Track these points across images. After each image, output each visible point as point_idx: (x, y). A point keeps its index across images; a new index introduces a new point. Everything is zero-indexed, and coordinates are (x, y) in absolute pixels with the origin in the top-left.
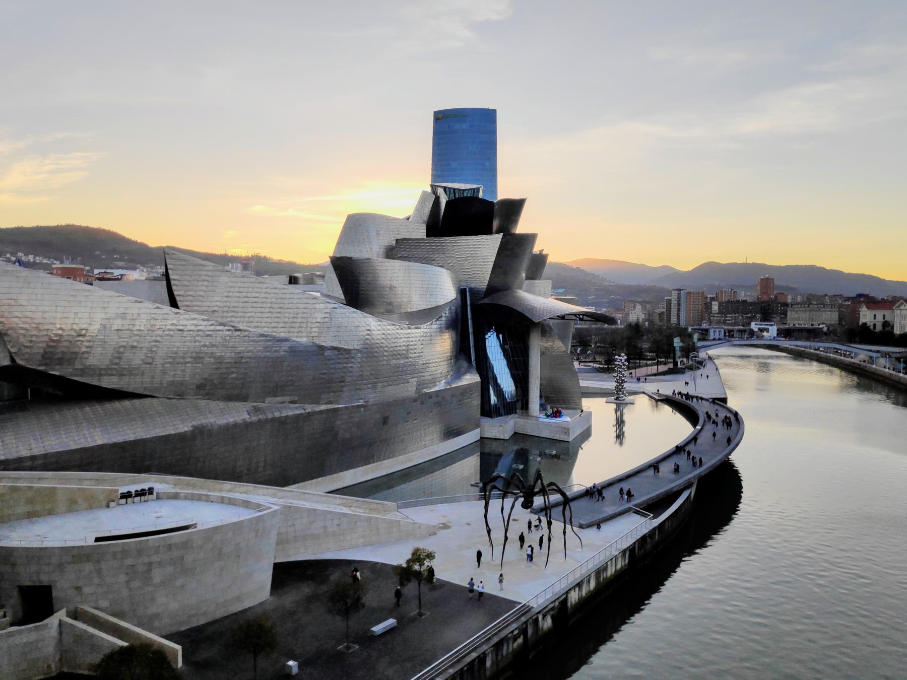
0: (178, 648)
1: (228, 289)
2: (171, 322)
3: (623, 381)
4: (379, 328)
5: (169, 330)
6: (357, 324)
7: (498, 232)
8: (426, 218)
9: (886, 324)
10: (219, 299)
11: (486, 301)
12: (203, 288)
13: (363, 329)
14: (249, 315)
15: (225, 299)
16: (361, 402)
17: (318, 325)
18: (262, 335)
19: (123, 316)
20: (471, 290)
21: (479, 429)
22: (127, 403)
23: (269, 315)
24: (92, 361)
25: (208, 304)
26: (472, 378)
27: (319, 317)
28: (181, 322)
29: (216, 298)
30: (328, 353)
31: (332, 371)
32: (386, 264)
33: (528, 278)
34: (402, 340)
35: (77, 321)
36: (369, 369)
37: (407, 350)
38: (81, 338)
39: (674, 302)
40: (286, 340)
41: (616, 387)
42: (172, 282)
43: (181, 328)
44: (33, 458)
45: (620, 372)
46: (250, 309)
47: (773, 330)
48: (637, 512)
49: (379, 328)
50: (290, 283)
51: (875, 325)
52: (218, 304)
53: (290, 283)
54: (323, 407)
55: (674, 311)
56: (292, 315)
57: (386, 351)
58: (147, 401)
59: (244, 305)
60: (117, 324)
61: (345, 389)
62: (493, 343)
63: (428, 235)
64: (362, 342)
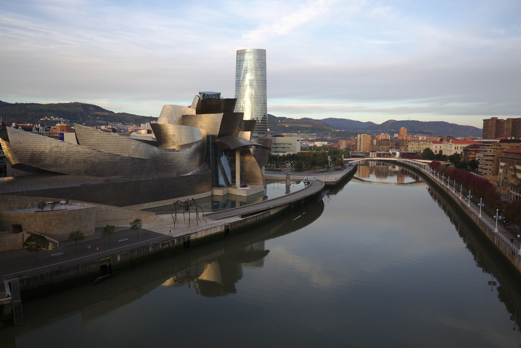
0: (57, 242)
9: (441, 151)
11: (218, 140)
16: (150, 179)
18: (109, 154)
19: (57, 147)
22: (59, 177)
24: (47, 162)
27: (133, 147)
30: (136, 160)
40: (119, 155)
44: (23, 192)
47: (398, 154)
50: (148, 133)
53: (148, 133)
55: (358, 144)
58: (66, 176)
60: (55, 149)
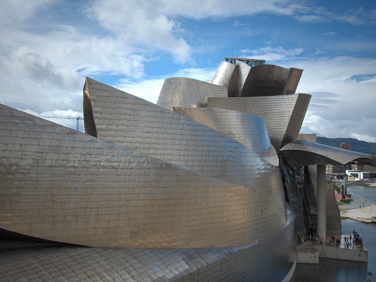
1: (148, 124)
2: (104, 158)
5: (104, 167)
8: (227, 83)
10: (141, 134)
12: (125, 122)
14: (168, 152)
15: (146, 135)
23: (186, 152)
25: (130, 139)
28: (115, 159)
29: (137, 134)
32: (225, 114)
35: (7, 154)
38: (11, 176)
42: (95, 115)
43: (115, 164)
46: (170, 147)
47: (361, 175)
49: (263, 167)
52: (140, 139)
56: (205, 153)
59: (165, 141)
63: (228, 96)
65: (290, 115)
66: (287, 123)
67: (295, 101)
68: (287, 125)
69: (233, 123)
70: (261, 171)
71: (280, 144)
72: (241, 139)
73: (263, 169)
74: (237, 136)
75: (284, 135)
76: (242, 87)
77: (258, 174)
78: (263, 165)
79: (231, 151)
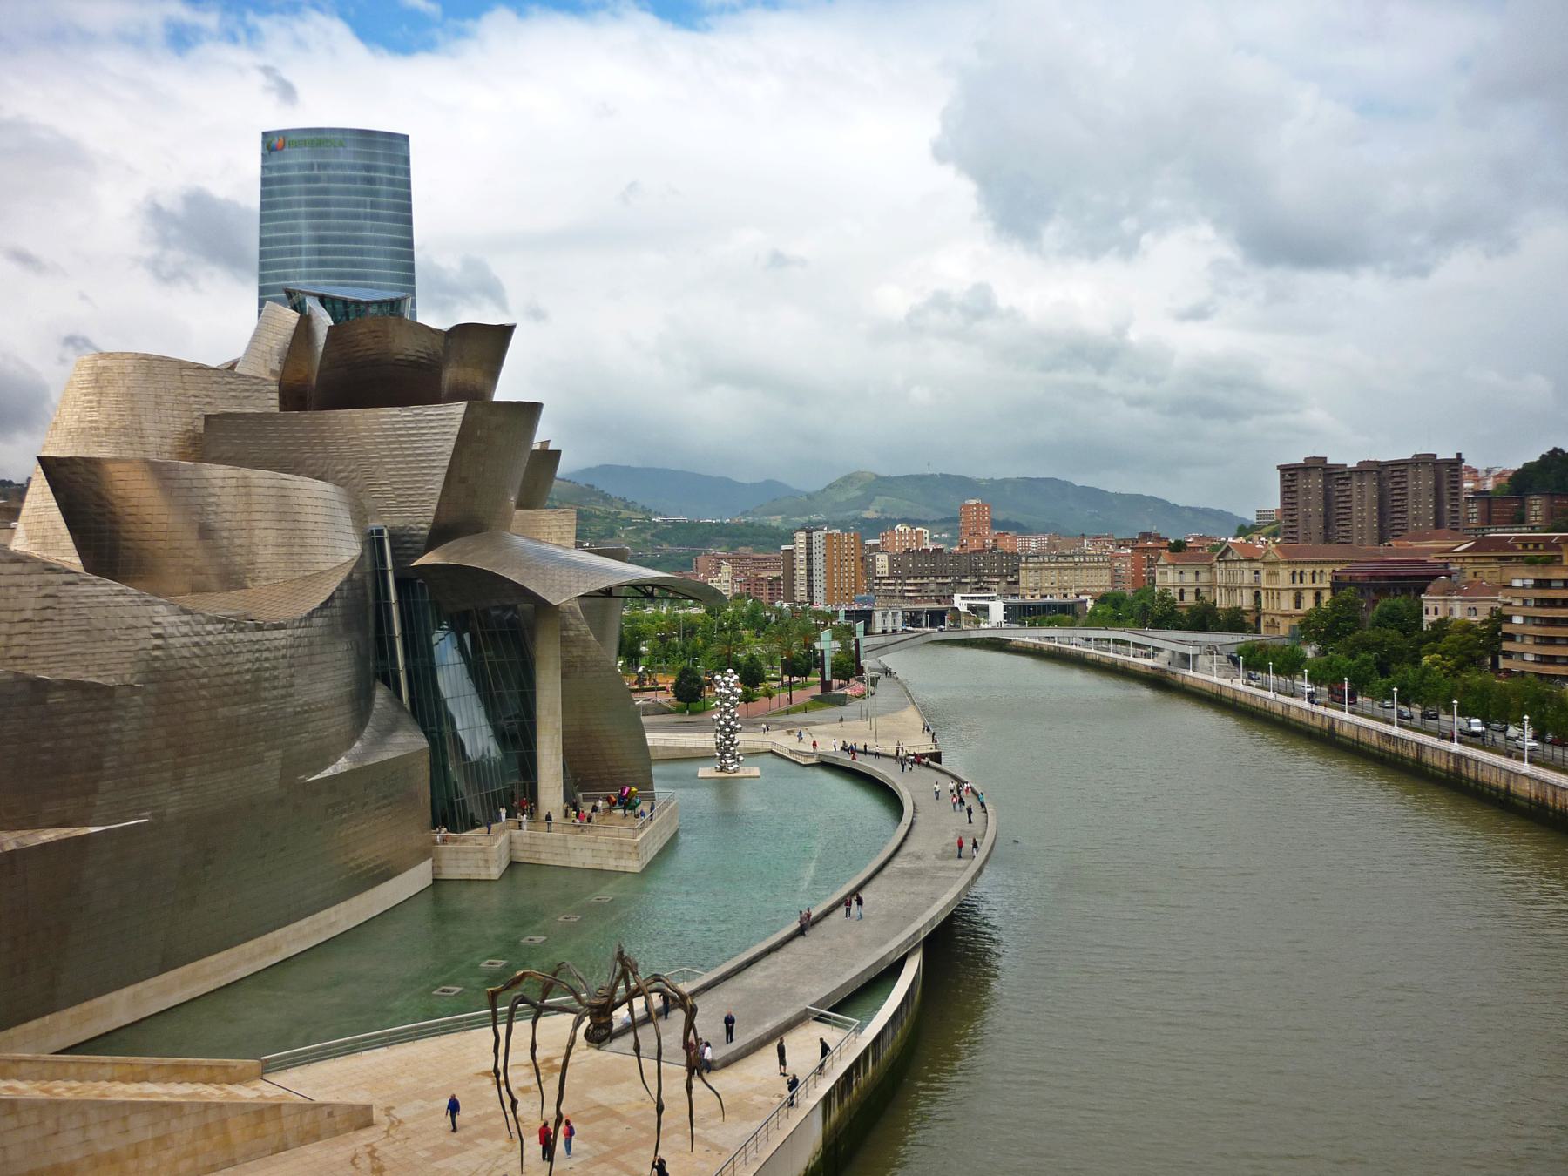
3: (734, 731)
4: (185, 629)
6: (130, 621)
7: (454, 397)
11: (430, 558)
13: (145, 633)
17: (25, 627)
20: (397, 537)
21: (428, 864)
26: (409, 742)
31: (68, 743)
33: (520, 505)
34: (241, 659)
36: (161, 732)
37: (257, 681)
39: (801, 554)
41: (718, 746)
45: (727, 711)
47: (997, 610)
48: (821, 1019)
49: (185, 629)
51: (1182, 593)
54: (48, 836)
55: (801, 572)
57: (203, 686)
61: (104, 786)
62: (447, 654)
64: (142, 666)
65: (447, 464)
66: (439, 486)
67: (458, 424)
68: (439, 492)
69: (212, 499)
70: (171, 641)
71: (422, 546)
72: (237, 542)
73: (186, 635)
74: (225, 534)
75: (431, 520)
76: (314, 381)
77: (157, 647)
78: (187, 623)
79: (46, 596)
